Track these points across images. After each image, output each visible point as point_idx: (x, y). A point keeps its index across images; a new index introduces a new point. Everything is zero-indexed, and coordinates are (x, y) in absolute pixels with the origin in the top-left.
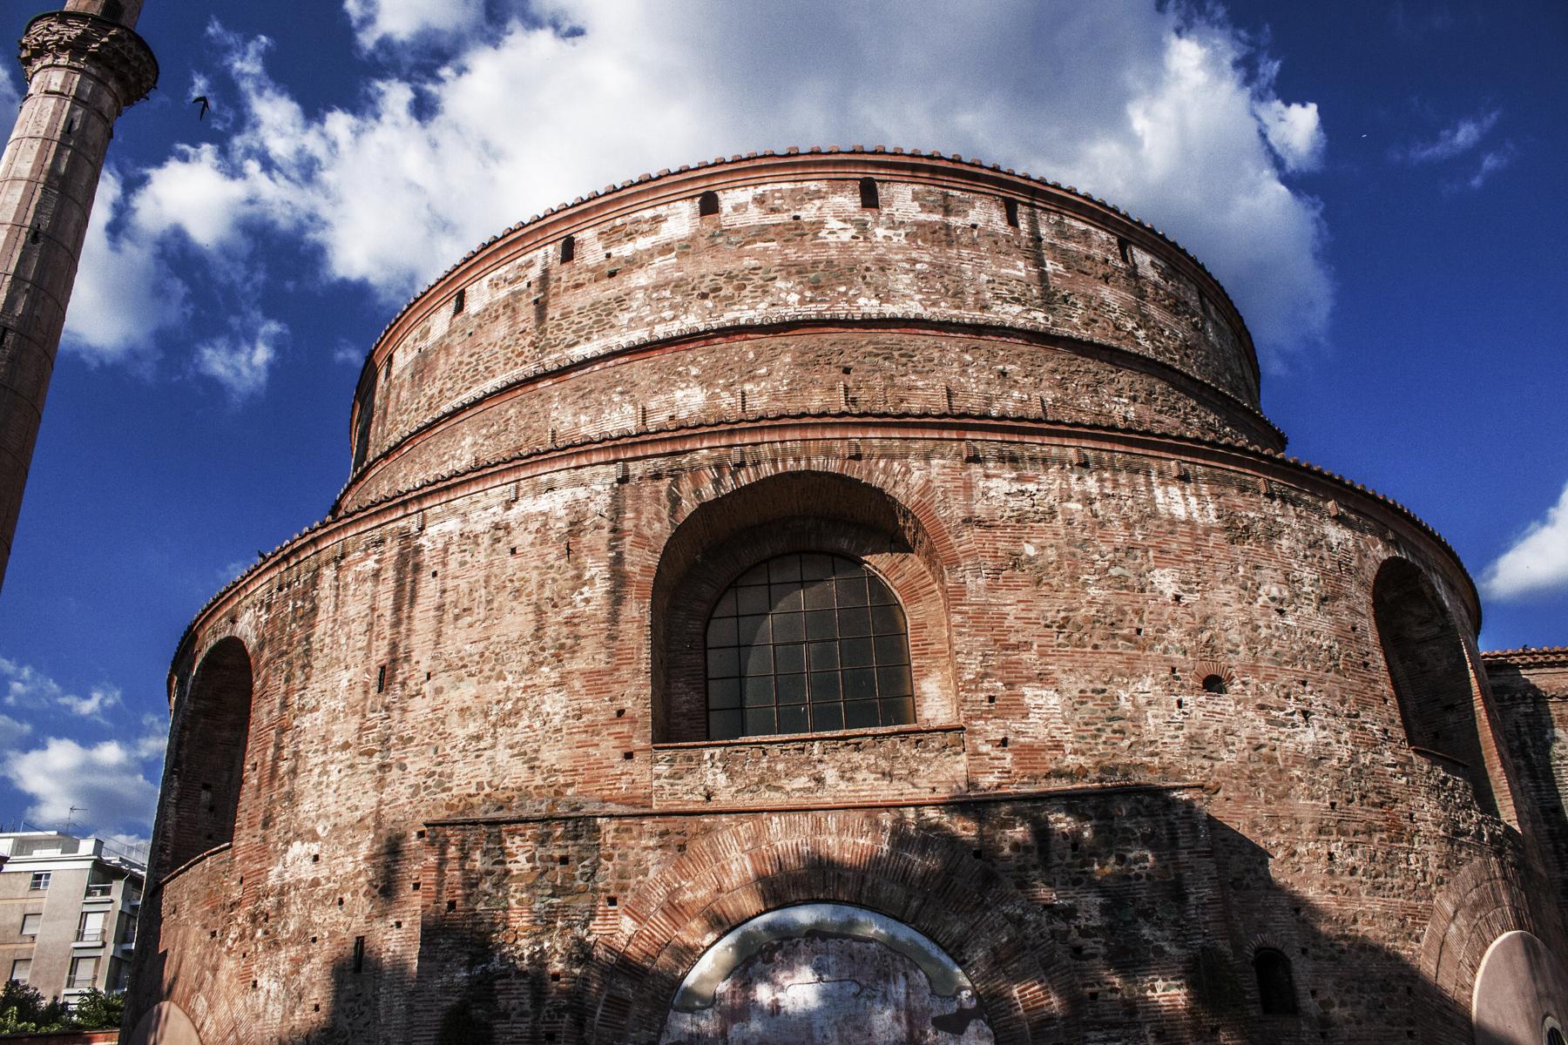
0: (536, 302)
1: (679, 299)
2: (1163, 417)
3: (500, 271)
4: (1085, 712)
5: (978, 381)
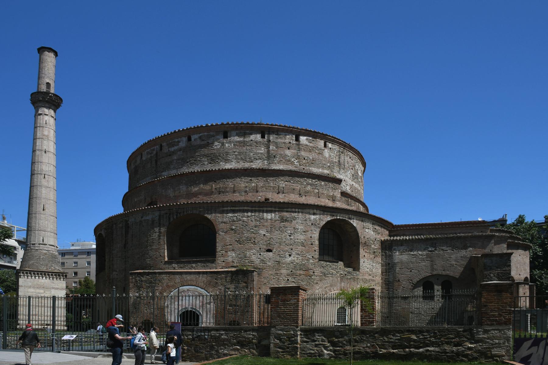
2: (293, 185)
3: (148, 150)
4: (239, 256)
5: (244, 182)
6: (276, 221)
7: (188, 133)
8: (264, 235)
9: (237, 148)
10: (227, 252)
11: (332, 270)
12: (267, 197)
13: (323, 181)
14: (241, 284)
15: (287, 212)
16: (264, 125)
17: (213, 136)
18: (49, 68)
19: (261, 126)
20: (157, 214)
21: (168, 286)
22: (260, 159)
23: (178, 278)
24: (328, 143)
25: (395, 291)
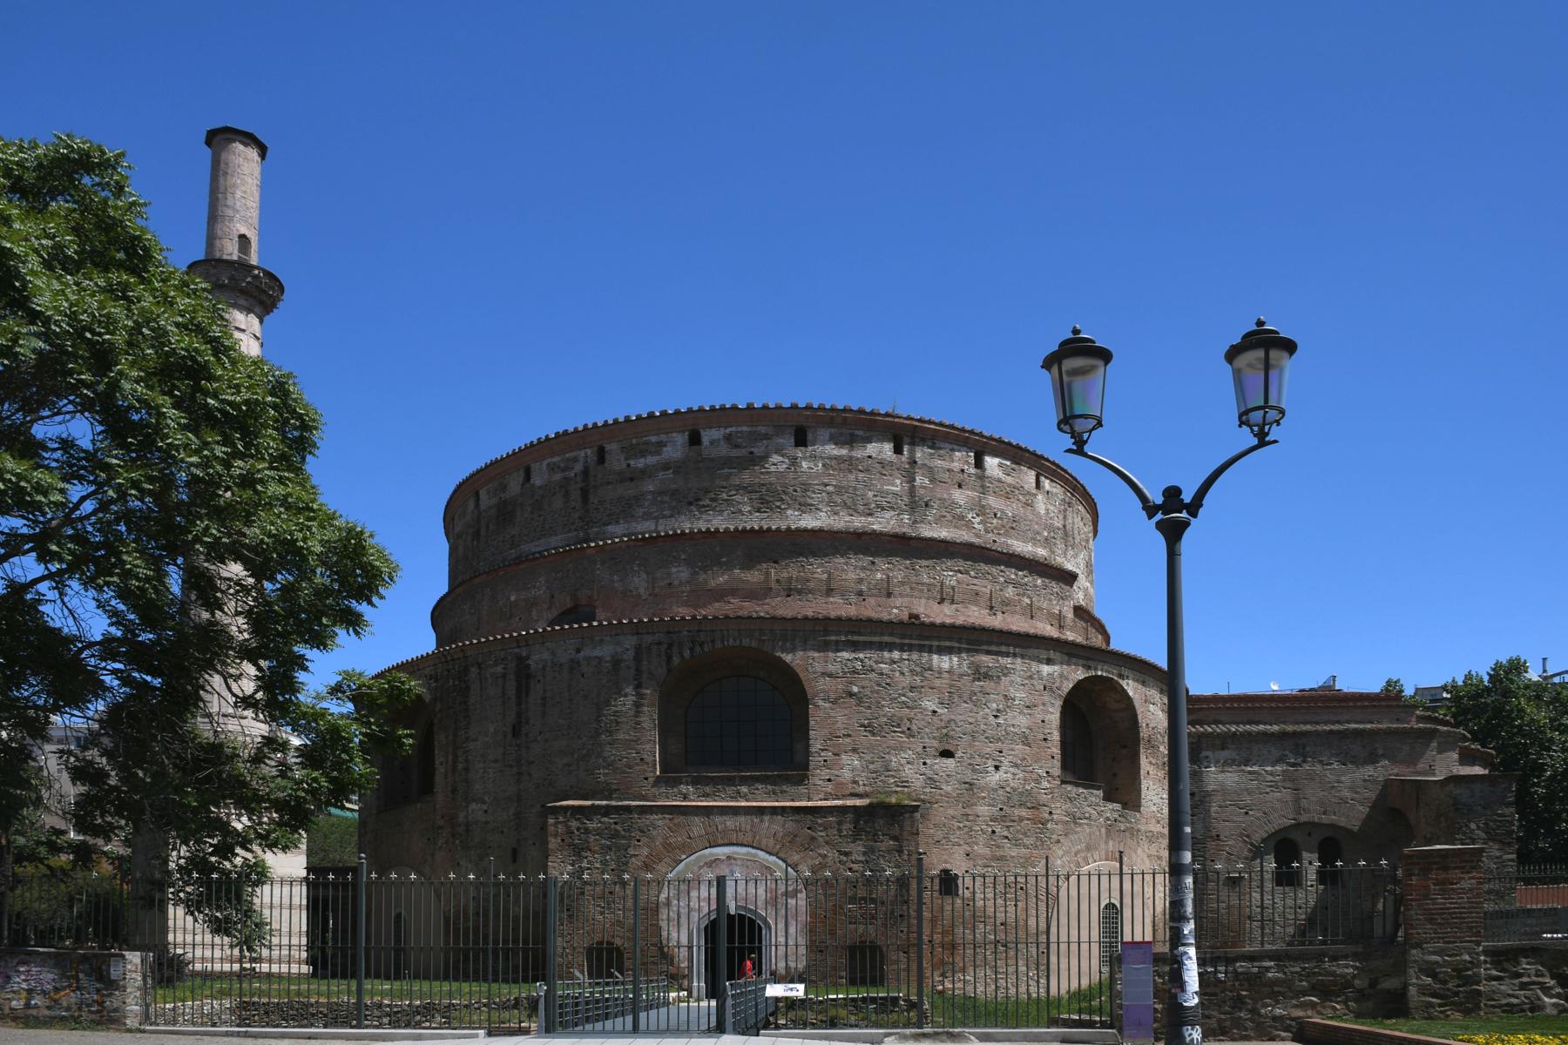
0: (581, 489)
1: (674, 504)
2: (976, 581)
3: (554, 460)
4: (871, 767)
5: (856, 567)
6: (961, 675)
7: (692, 424)
8: (935, 712)
9: (833, 475)
10: (838, 755)
11: (1089, 809)
12: (915, 612)
13: (1041, 575)
14: (882, 841)
15: (988, 653)
16: (902, 421)
17: (766, 437)
18: (245, 192)
19: (896, 420)
20: (630, 642)
21: (668, 847)
22: (892, 508)
23: (697, 825)
24: (1042, 479)
25: (1208, 863)
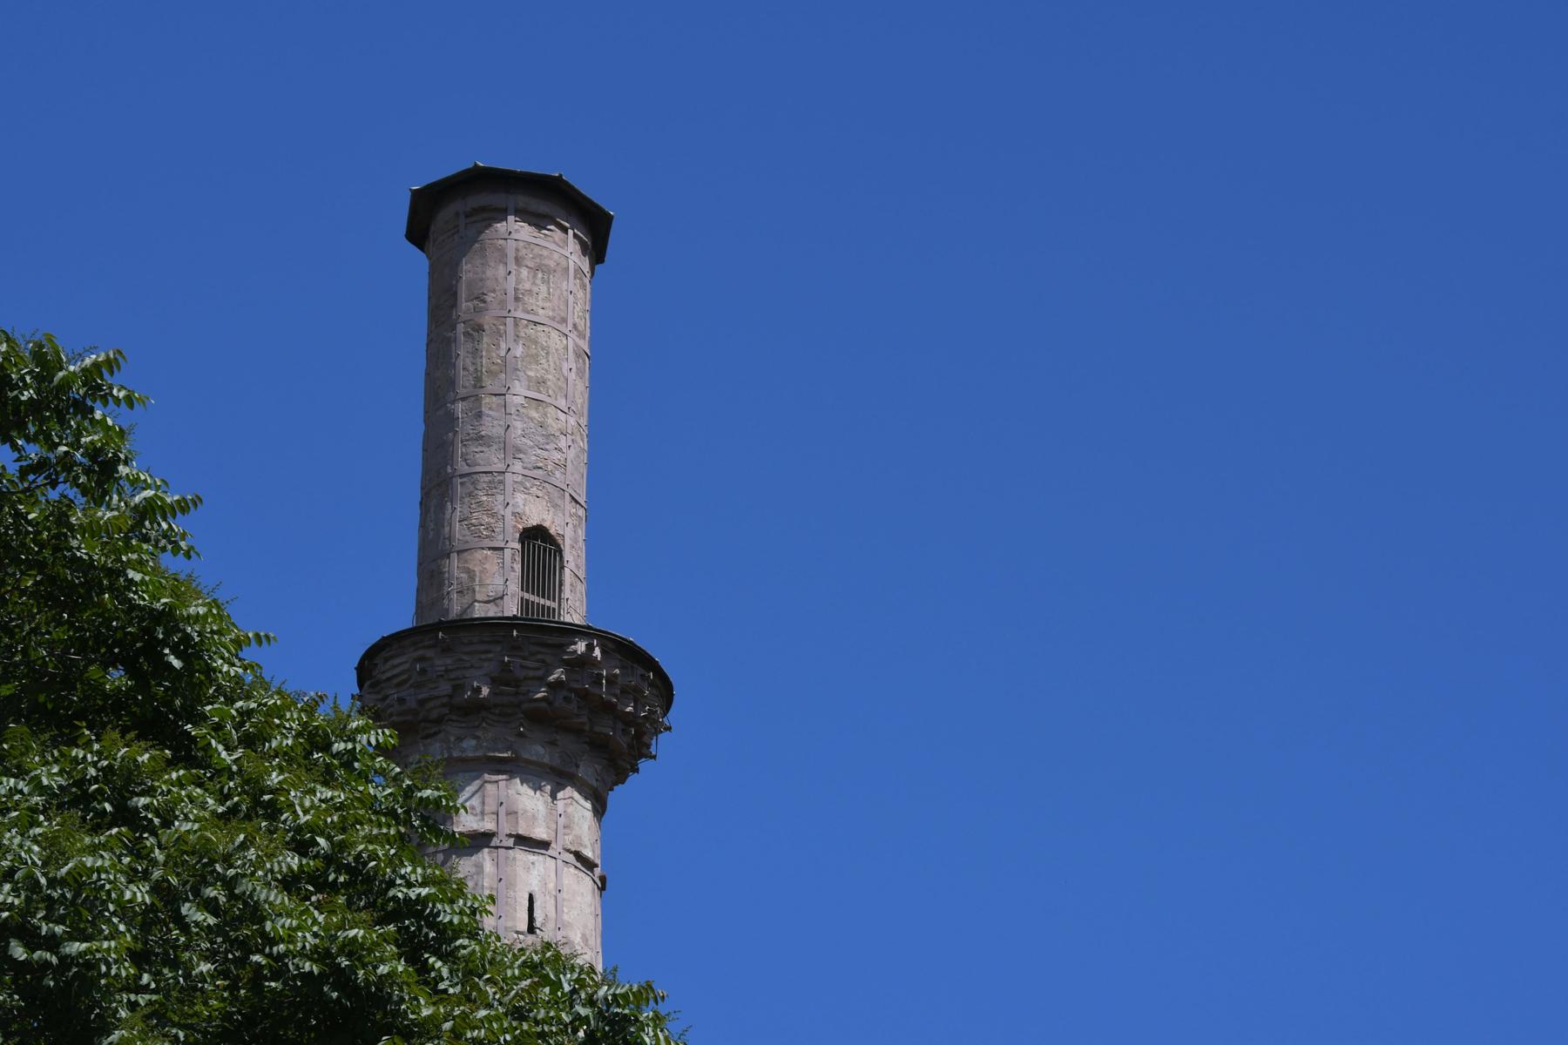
18: (540, 383)
